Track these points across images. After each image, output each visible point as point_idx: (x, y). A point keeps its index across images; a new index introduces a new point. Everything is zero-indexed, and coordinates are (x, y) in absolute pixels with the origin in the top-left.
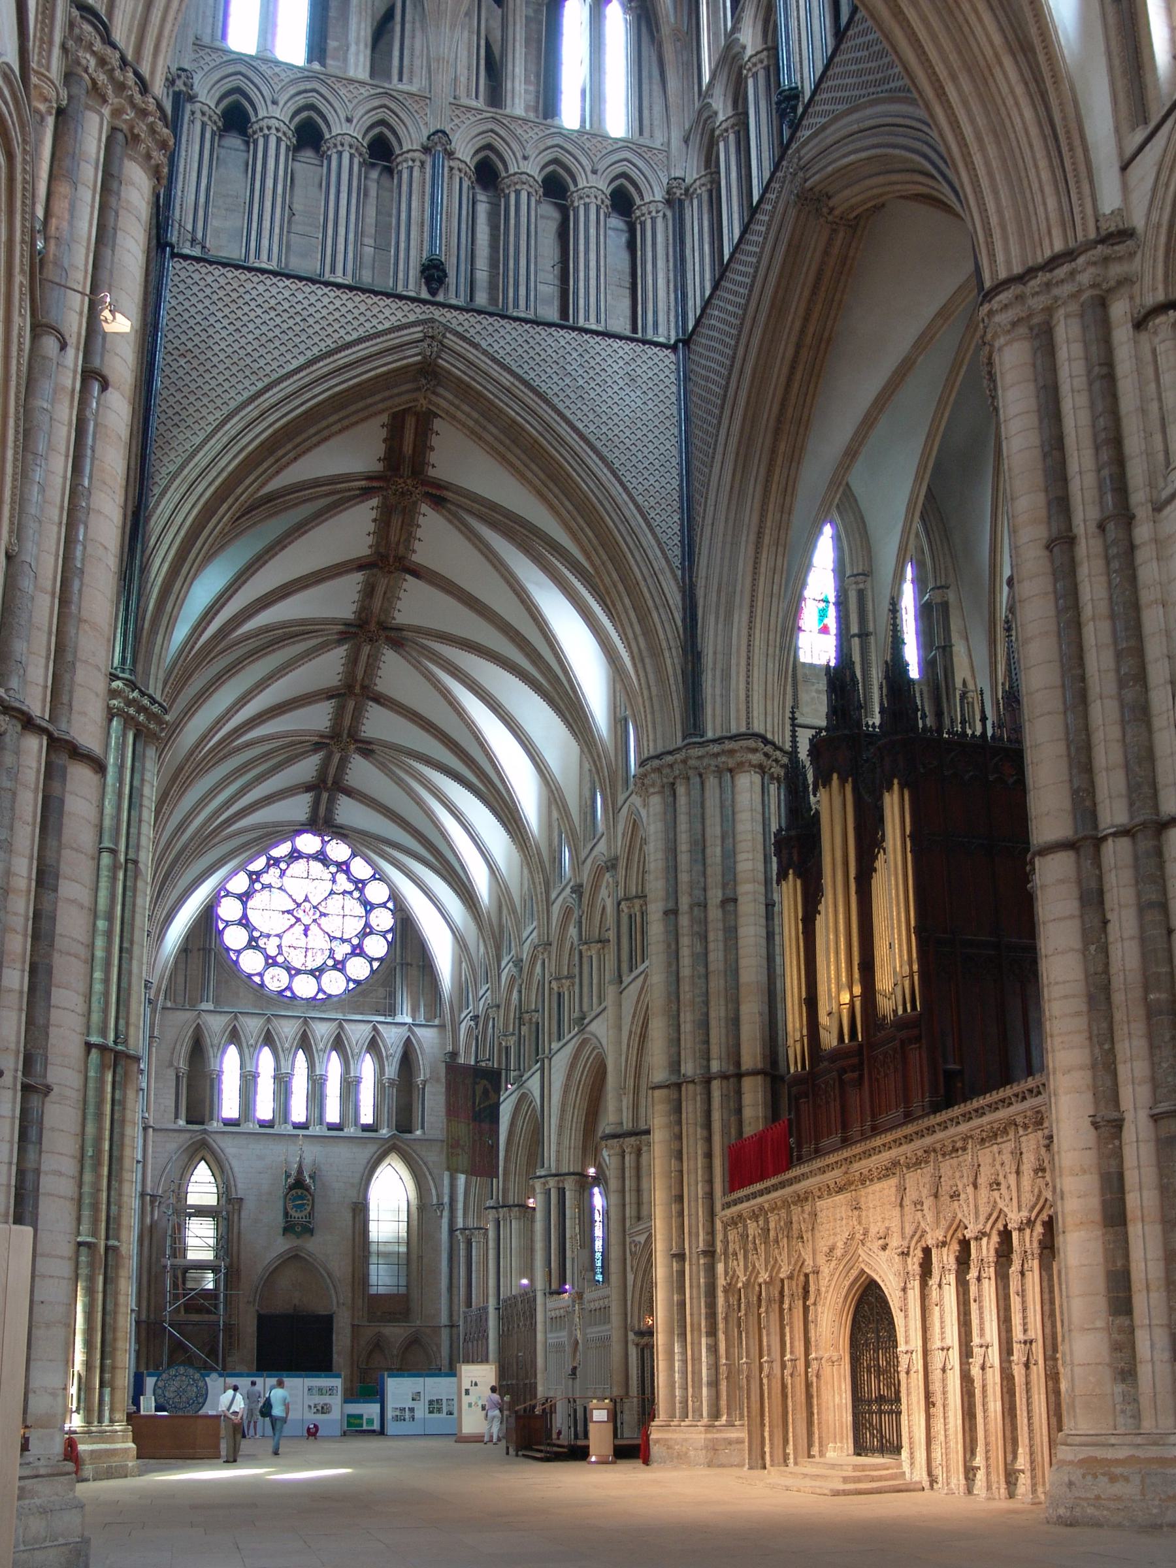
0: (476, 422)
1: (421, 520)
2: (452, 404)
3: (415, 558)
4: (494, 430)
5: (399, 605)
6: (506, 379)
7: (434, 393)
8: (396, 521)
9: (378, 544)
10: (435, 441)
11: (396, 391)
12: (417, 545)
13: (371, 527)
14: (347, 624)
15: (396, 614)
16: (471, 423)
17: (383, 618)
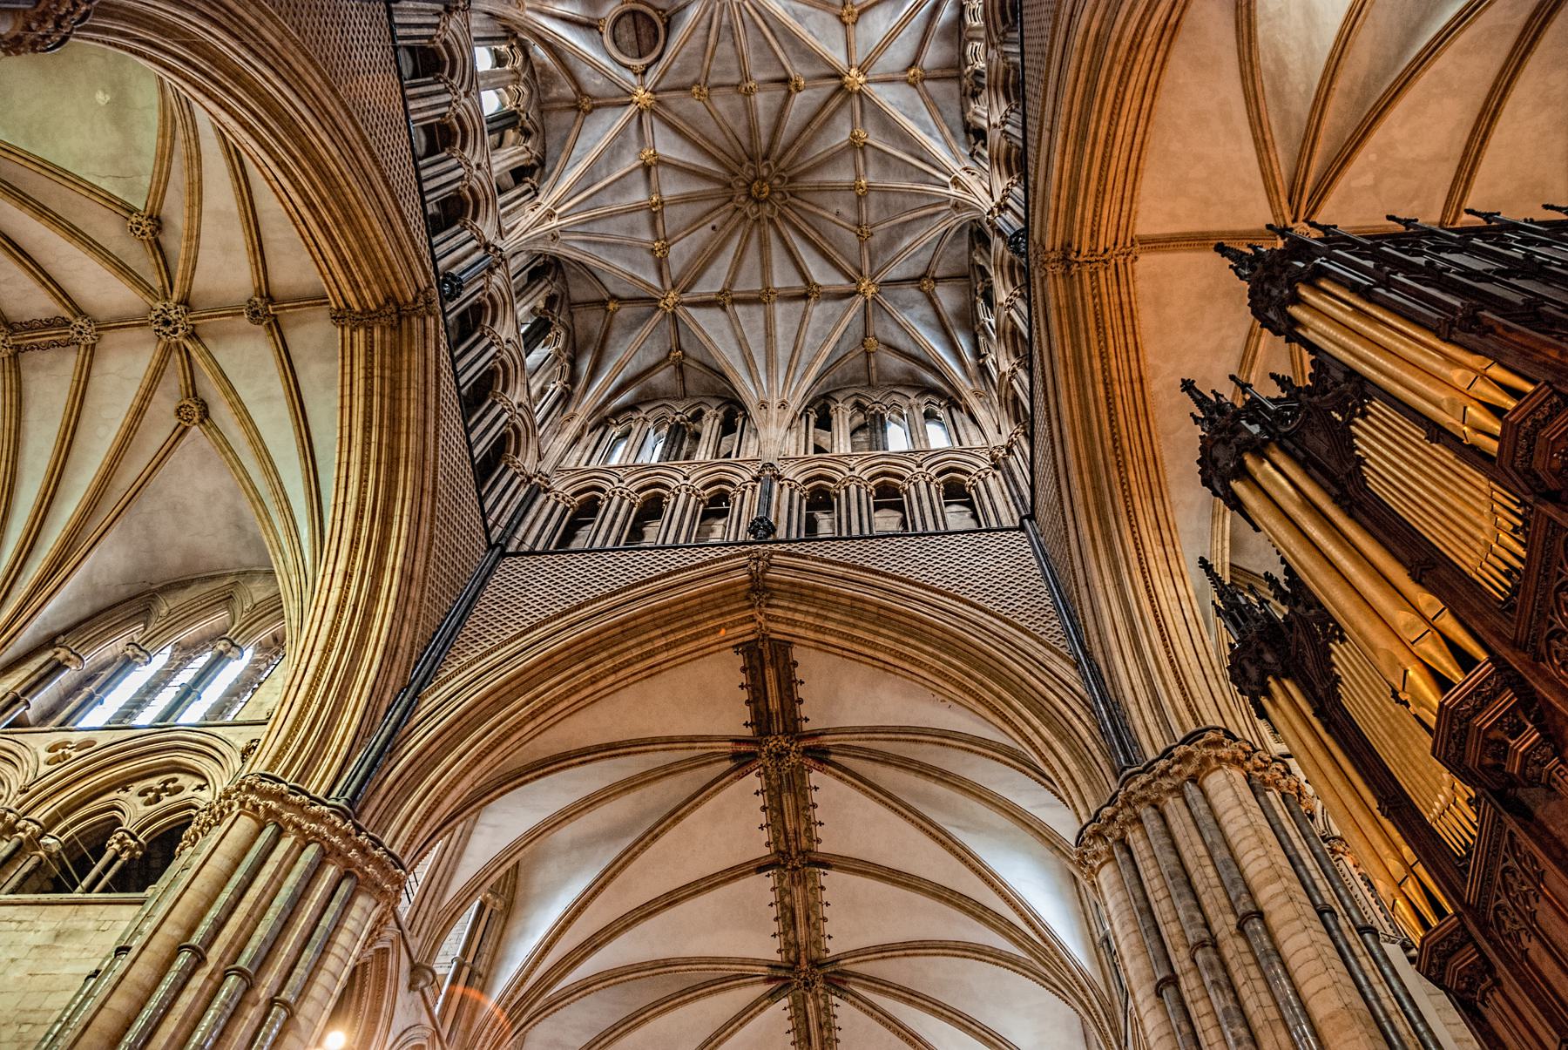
0: (817, 615)
1: (815, 797)
2: (789, 609)
3: (821, 848)
4: (837, 616)
5: (828, 928)
6: (839, 571)
7: (768, 606)
8: (788, 801)
9: (776, 840)
10: (801, 692)
11: (726, 609)
12: (819, 832)
13: (763, 818)
14: (773, 966)
15: (828, 944)
16: (810, 620)
17: (814, 953)
